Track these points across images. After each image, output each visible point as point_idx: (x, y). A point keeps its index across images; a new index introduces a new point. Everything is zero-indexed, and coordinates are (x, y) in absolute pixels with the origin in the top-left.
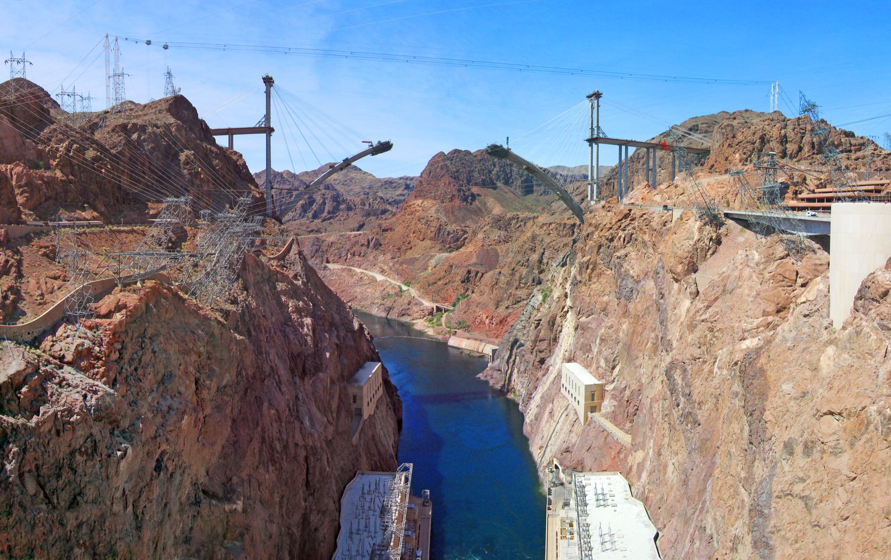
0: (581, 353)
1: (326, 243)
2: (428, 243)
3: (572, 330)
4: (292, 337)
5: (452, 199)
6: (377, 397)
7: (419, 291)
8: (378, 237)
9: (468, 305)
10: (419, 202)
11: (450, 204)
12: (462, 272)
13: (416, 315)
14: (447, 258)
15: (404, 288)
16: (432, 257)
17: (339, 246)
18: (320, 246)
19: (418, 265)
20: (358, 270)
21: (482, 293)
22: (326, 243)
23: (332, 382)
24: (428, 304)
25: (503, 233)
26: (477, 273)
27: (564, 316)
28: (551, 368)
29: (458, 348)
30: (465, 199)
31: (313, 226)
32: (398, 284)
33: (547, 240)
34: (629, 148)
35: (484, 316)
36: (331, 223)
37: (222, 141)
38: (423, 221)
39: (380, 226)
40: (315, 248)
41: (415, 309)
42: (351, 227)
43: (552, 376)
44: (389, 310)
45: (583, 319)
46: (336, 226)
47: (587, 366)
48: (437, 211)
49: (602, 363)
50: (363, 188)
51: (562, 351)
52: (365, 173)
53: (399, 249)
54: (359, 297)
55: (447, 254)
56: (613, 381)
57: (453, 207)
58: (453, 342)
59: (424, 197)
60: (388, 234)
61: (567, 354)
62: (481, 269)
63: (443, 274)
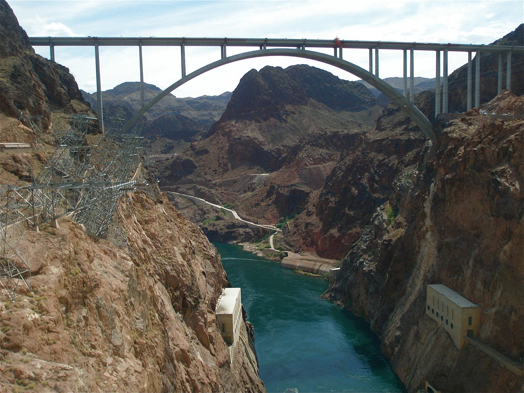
0: (449, 273)
3: (434, 251)
8: (191, 159)
9: (296, 226)
12: (285, 192)
21: (309, 214)
25: (323, 151)
27: (422, 237)
28: (409, 289)
30: (280, 118)
33: (381, 157)
37: (42, 51)
39: (192, 147)
41: (241, 231)
43: (412, 298)
45: (448, 240)
47: (458, 289)
49: (479, 285)
51: (422, 272)
53: (215, 171)
55: (268, 174)
56: (494, 306)
60: (204, 157)
61: (429, 276)
62: (305, 189)
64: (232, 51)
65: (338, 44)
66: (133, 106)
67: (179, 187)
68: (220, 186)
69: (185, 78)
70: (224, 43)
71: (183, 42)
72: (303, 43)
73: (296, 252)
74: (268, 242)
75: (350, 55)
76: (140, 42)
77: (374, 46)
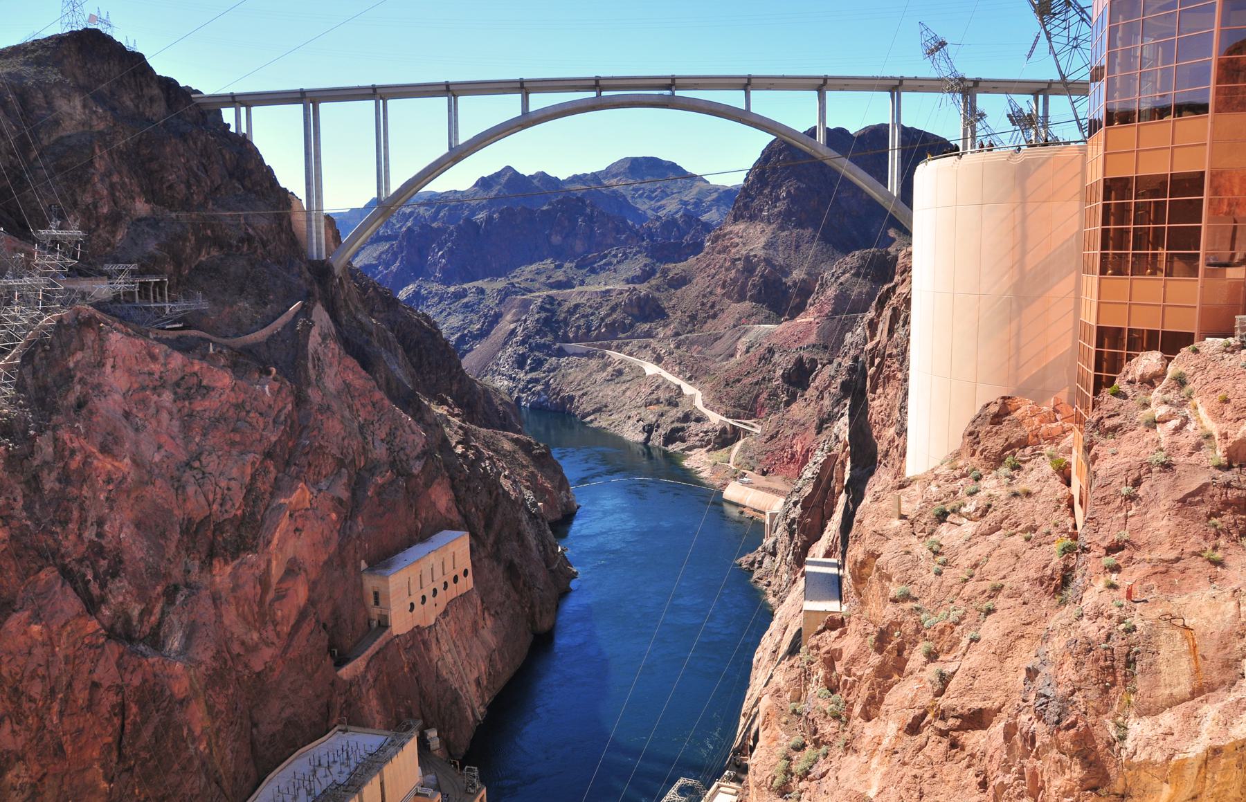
1: (565, 307)
2: (747, 305)
4: (191, 490)
5: (800, 225)
6: (443, 598)
7: (708, 395)
8: (657, 294)
10: (740, 227)
11: (796, 231)
13: (693, 441)
14: (769, 335)
15: (688, 389)
16: (746, 331)
17: (590, 311)
18: (553, 312)
19: (719, 346)
20: (615, 355)
22: (565, 307)
23: (292, 569)
24: (716, 419)
26: (814, 362)
29: (737, 505)
31: (559, 276)
32: (677, 381)
34: (1052, 98)
35: (798, 448)
36: (593, 271)
38: (740, 265)
40: (544, 315)
41: (693, 427)
42: (631, 274)
44: (649, 429)
46: (603, 276)
48: (769, 245)
50: (685, 203)
52: (693, 177)
53: (693, 318)
54: (611, 406)
57: (799, 237)
58: (733, 492)
59: (752, 218)
63: (754, 363)
64: (539, 101)
65: (747, 84)
66: (629, 199)
67: (627, 344)
68: (692, 343)
69: (457, 154)
70: (523, 87)
71: (450, 90)
72: (669, 82)
73: (764, 474)
74: (730, 451)
75: (764, 103)
76: (378, 94)
77: (822, 85)
